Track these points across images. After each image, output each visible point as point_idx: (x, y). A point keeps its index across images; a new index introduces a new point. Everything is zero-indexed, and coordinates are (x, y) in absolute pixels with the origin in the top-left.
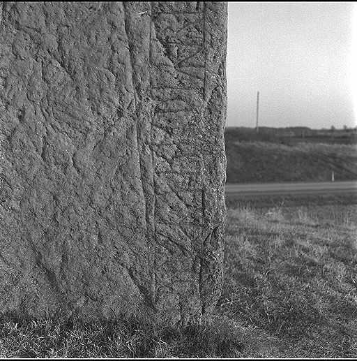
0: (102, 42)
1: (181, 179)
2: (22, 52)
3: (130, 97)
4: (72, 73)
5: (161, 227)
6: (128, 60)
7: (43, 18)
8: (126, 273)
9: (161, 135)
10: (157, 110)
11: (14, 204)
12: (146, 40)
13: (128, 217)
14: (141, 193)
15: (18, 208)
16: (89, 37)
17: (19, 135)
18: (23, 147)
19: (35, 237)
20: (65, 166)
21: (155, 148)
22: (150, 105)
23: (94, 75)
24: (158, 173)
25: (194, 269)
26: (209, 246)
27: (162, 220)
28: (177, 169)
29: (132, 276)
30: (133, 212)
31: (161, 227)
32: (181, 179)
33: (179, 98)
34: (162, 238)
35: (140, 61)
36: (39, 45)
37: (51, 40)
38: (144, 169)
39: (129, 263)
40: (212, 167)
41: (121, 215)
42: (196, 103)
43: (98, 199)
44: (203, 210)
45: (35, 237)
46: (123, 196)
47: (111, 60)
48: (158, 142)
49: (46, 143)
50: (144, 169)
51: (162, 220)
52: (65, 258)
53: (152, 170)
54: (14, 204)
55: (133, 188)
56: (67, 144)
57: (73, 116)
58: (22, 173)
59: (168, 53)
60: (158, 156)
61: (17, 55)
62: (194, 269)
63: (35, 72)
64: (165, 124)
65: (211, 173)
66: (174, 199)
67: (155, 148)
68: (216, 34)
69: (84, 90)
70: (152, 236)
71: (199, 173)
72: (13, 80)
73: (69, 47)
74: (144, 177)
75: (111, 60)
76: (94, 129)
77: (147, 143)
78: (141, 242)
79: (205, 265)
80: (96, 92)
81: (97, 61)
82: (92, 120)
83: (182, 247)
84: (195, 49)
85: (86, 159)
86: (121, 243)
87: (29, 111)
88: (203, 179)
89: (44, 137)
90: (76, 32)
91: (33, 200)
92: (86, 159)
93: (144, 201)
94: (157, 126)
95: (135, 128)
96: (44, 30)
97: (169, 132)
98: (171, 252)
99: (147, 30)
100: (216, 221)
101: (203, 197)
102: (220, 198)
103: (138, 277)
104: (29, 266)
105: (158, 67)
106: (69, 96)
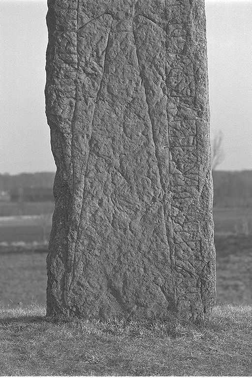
0: (144, 163)
1: (188, 235)
2: (101, 169)
3: (160, 191)
4: (127, 178)
5: (178, 262)
6: (158, 172)
7: (111, 150)
8: (160, 289)
10: (174, 198)
12: (167, 161)
13: (161, 257)
14: (167, 243)
15: (99, 255)
16: (137, 160)
17: (99, 214)
19: (109, 270)
21: (174, 218)
23: (140, 180)
24: (176, 232)
25: (197, 285)
26: (205, 272)
27: (179, 258)
28: (186, 229)
29: (163, 292)
30: (163, 254)
31: (178, 262)
32: (188, 235)
33: (185, 191)
34: (179, 268)
35: (164, 172)
36: (110, 165)
37: (117, 162)
38: (168, 230)
40: (205, 228)
42: (195, 194)
43: (143, 248)
44: (201, 251)
45: (109, 270)
46: (157, 245)
47: (148, 172)
48: (175, 215)
49: (114, 217)
50: (168, 230)
51: (179, 258)
52: (125, 282)
53: (172, 231)
55: (162, 241)
56: (126, 218)
57: (129, 203)
58: (101, 234)
59: (179, 168)
60: (175, 222)
61: (98, 170)
62: (197, 285)
63: (108, 179)
64: (178, 205)
65: (204, 231)
66: (184, 246)
67: (174, 218)
68: (203, 157)
69: (135, 188)
70: (174, 268)
71: (198, 231)
72: (96, 183)
73: (126, 165)
74: (168, 235)
75: (148, 172)
76: (141, 209)
77: (169, 215)
78: (168, 271)
79: (204, 283)
80: (141, 189)
81: (141, 173)
82: (140, 205)
83: (190, 273)
84: (192, 165)
85: (137, 225)
86: (157, 272)
87: (105, 200)
88: (201, 234)
89: (113, 214)
90: (130, 157)
91: (107, 249)
92: (137, 225)
93: (169, 248)
94: (174, 206)
95: (163, 208)
96: (112, 157)
97: (181, 209)
98: (184, 276)
99: (167, 155)
100: (209, 258)
101: (201, 244)
102: (210, 245)
103: (167, 291)
104: (105, 288)
105: (174, 175)
106: (126, 191)
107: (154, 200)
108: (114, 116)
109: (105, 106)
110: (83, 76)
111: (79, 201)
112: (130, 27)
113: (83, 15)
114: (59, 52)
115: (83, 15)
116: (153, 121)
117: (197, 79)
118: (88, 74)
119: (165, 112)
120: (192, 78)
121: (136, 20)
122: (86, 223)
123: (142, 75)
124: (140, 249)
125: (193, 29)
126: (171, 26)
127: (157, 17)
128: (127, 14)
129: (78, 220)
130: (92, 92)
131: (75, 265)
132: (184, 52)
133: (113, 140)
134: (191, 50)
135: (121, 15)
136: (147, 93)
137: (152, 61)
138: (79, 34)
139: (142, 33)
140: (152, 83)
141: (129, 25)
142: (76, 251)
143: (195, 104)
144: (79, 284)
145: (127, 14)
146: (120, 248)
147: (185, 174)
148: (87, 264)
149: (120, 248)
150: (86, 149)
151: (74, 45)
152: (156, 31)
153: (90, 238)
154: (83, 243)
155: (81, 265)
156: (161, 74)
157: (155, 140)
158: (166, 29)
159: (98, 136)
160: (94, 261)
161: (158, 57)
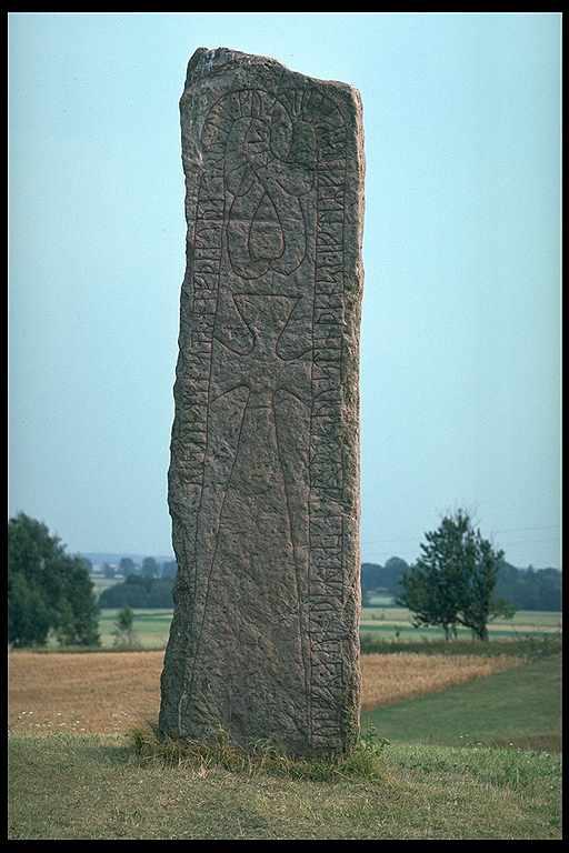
27: (315, 684)
39: (293, 712)
51: (315, 684)
57: (260, 613)
85: (268, 643)
86: (288, 700)
96: (243, 556)
108: (246, 507)
113: (216, 386)
115: (216, 386)
116: (291, 517)
117: (344, 467)
119: (306, 505)
137: (292, 442)
139: (282, 409)
140: (292, 470)
156: (303, 460)
161: (300, 439)
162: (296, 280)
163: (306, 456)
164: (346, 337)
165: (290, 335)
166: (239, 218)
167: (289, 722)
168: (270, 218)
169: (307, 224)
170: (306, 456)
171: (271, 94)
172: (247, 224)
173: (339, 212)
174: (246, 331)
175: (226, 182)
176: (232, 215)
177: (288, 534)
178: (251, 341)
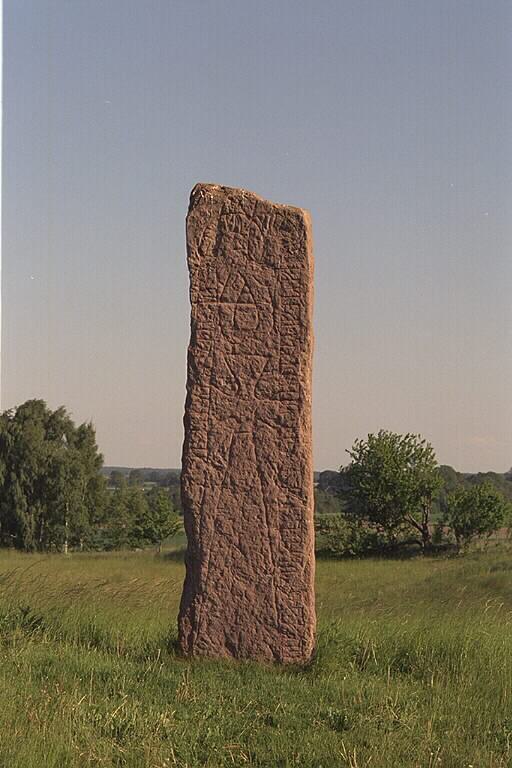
0: (258, 541)
9: (284, 583)
11: (218, 614)
12: (277, 541)
18: (222, 587)
20: (241, 596)
22: (278, 570)
30: (272, 618)
35: (275, 550)
36: (231, 542)
38: (277, 598)
40: (307, 599)
41: (265, 619)
50: (277, 598)
52: (240, 640)
54: (218, 614)
55: (271, 607)
59: (286, 547)
61: (221, 546)
72: (219, 557)
73: (244, 543)
74: (276, 602)
78: (275, 632)
79: (304, 643)
80: (255, 563)
83: (294, 635)
85: (251, 594)
97: (287, 581)
105: (282, 553)
107: (266, 573)
108: (234, 501)
109: (228, 493)
110: (211, 468)
111: (204, 570)
112: (250, 429)
113: (213, 417)
114: (192, 448)
115: (213, 417)
116: (266, 507)
117: (303, 473)
118: (215, 466)
120: (299, 473)
121: (255, 424)
122: (210, 590)
123: (259, 469)
124: (253, 613)
125: (301, 432)
126: (283, 430)
127: (272, 422)
128: (248, 419)
129: (203, 586)
130: (218, 482)
131: (200, 625)
132: (293, 451)
133: (234, 521)
134: (299, 450)
135: (243, 419)
136: (262, 484)
138: (209, 434)
139: (260, 434)
140: (266, 475)
141: (249, 426)
142: (201, 612)
143: (301, 496)
144: (202, 639)
145: (248, 419)
146: (236, 612)
147: (291, 551)
148: (210, 623)
149: (236, 612)
150: (211, 527)
151: (204, 442)
152: (271, 433)
153: (213, 601)
154: (207, 606)
155: (205, 625)
156: (273, 468)
157: (268, 523)
158: (279, 432)
159: (221, 518)
160: (216, 621)
162: (267, 345)
163: (276, 466)
164: (301, 383)
165: (263, 382)
166: (227, 301)
167: (267, 649)
168: (249, 302)
169: (275, 306)
170: (276, 466)
171: (248, 216)
172: (233, 305)
173: (297, 298)
174: (233, 380)
175: (218, 277)
176: (223, 299)
177: (265, 520)
178: (237, 387)
